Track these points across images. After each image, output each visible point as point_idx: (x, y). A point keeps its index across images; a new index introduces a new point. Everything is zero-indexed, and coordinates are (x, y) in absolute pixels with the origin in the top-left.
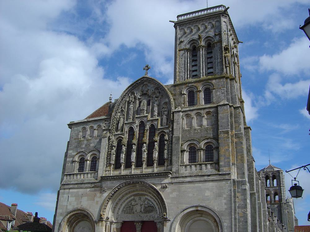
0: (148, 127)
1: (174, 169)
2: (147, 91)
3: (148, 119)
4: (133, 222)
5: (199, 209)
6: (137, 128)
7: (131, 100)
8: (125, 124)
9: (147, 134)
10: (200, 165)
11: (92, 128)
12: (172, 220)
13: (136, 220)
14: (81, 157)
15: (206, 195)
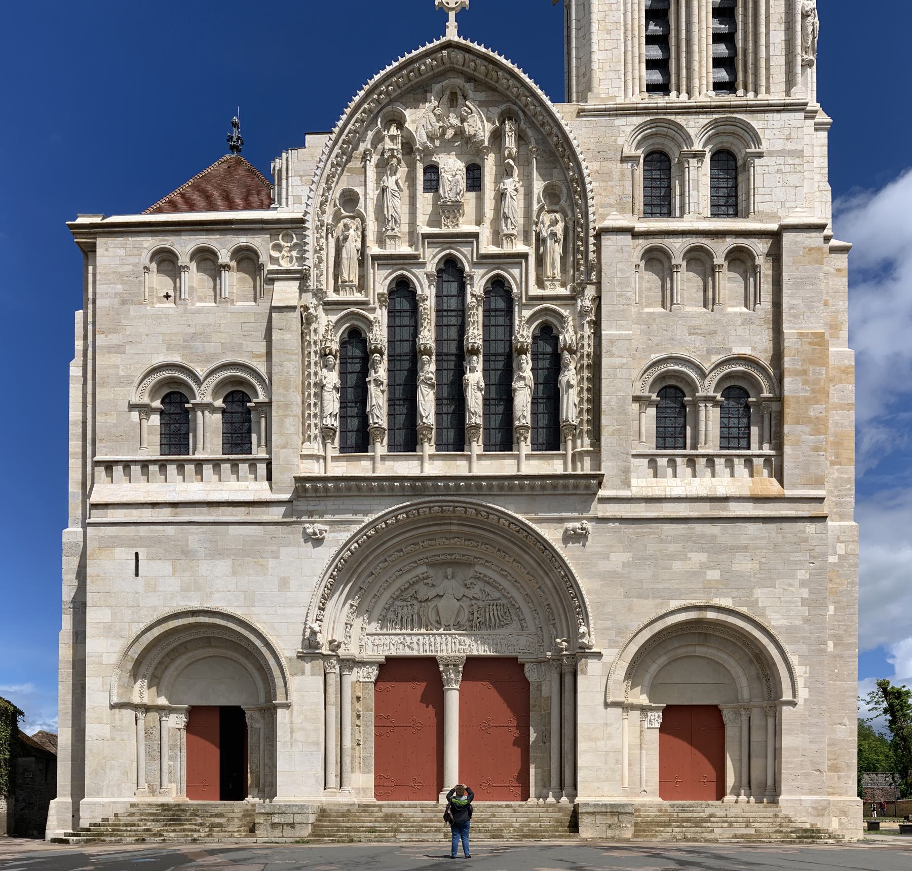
0: (478, 284)
1: (607, 468)
2: (463, 121)
3: (483, 251)
4: (431, 662)
5: (711, 615)
6: (429, 286)
7: (392, 150)
8: (375, 258)
9: (477, 317)
10: (710, 460)
11: (205, 259)
12: (609, 655)
13: (444, 654)
14: (168, 391)
15: (736, 567)
